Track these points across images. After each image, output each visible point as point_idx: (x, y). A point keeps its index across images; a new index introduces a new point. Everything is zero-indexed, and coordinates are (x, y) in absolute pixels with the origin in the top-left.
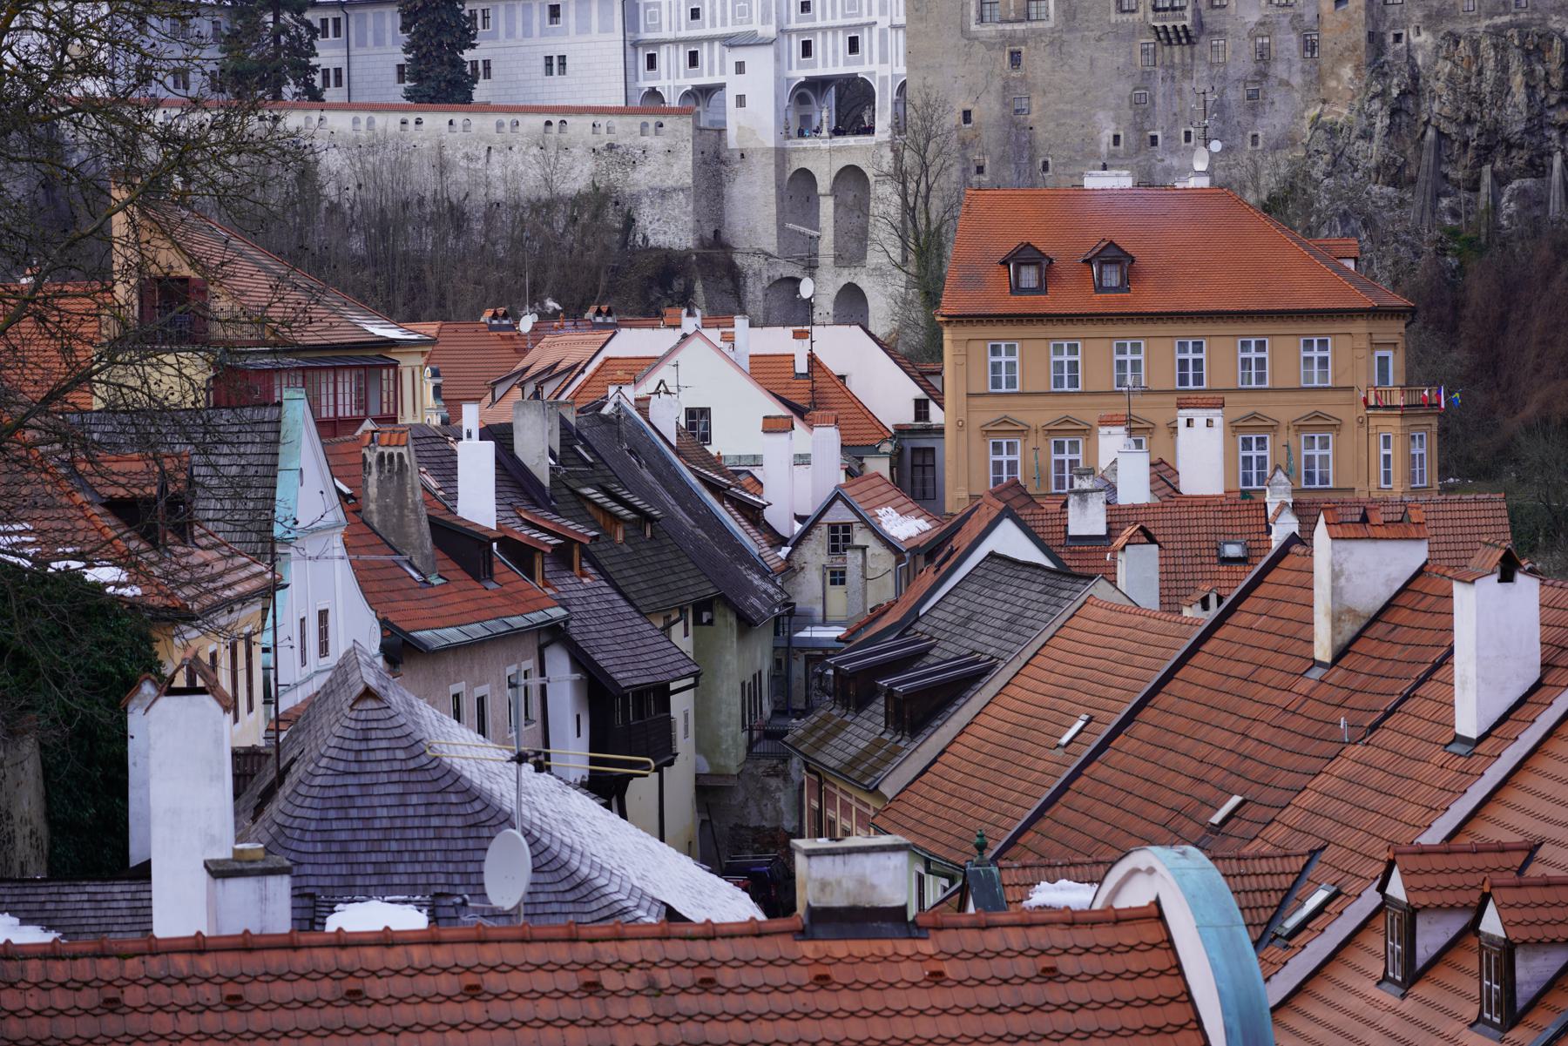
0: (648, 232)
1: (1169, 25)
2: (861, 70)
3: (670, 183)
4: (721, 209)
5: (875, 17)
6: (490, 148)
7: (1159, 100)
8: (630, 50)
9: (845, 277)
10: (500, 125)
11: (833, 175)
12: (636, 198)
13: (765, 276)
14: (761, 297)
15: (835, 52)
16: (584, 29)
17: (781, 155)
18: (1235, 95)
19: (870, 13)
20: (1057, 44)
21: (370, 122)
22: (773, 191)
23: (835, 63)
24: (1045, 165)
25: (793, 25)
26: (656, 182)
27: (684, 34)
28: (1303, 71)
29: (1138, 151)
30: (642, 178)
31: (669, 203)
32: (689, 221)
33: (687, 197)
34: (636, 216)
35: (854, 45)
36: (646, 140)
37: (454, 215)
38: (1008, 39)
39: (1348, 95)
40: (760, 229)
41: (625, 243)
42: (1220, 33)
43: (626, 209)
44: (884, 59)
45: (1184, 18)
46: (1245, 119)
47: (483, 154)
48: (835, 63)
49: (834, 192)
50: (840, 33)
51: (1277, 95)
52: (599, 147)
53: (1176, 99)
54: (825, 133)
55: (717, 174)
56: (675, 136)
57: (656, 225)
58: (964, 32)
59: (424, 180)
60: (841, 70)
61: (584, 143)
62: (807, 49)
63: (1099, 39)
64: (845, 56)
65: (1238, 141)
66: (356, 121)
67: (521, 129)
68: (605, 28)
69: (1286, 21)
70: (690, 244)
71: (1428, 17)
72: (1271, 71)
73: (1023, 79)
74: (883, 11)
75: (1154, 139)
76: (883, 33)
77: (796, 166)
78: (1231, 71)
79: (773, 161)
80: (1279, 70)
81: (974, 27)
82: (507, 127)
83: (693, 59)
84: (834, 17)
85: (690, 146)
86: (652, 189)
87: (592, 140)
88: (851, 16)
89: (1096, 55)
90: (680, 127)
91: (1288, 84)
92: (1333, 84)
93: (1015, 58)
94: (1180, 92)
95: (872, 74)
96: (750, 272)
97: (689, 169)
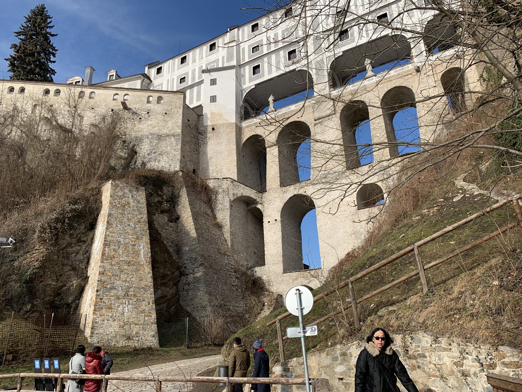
3: (165, 131)
4: (198, 158)
9: (292, 191)
10: (47, 92)
12: (140, 140)
13: (231, 192)
17: (239, 131)
22: (234, 147)
26: (156, 130)
33: (177, 140)
34: (138, 149)
43: (131, 145)
49: (279, 142)
56: (171, 105)
70: (178, 168)
79: (234, 130)
82: (52, 93)
86: (151, 134)
90: (174, 100)
96: (220, 190)
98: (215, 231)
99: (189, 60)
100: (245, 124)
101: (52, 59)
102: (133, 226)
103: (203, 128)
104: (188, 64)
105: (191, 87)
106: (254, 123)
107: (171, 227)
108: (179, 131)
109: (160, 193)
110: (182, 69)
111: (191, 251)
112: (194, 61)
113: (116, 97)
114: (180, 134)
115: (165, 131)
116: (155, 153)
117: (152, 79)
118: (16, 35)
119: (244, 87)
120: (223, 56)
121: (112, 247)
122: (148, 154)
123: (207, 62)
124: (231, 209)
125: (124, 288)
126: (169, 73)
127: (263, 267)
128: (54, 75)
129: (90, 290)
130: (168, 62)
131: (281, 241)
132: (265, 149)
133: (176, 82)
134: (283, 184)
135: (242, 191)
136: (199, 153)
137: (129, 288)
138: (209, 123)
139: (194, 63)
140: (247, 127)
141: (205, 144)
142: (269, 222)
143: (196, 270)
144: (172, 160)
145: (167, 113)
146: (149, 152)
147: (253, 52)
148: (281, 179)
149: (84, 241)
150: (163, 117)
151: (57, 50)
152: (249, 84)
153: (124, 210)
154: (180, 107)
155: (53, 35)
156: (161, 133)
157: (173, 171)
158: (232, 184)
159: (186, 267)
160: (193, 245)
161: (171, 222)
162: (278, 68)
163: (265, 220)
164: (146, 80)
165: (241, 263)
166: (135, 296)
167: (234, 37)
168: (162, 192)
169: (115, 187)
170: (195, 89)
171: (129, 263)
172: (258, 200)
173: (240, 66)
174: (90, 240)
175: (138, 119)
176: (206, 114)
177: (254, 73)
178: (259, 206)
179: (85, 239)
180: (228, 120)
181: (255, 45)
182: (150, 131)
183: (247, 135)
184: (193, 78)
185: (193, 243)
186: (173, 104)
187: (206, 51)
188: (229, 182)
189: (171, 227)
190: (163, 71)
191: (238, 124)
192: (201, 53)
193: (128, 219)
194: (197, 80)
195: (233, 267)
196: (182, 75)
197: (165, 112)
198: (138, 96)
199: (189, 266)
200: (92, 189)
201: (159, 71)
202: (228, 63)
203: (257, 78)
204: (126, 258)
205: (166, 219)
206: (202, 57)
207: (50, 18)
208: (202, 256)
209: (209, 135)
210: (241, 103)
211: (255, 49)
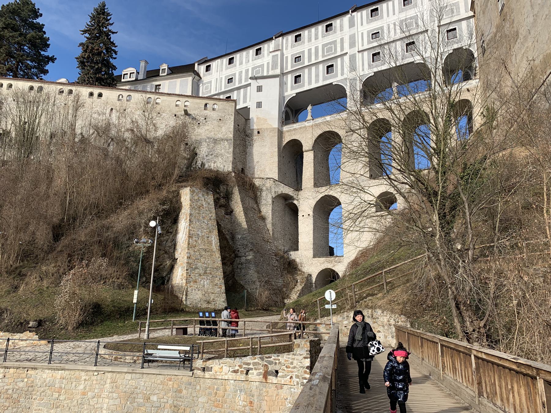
3: (220, 136)
4: (245, 158)
5: (347, 49)
6: (112, 109)
9: (324, 191)
11: (314, 139)
12: (199, 142)
13: (273, 190)
14: (270, 202)
17: (281, 134)
19: (342, 49)
22: (277, 149)
26: (212, 135)
27: (223, 90)
33: (230, 144)
40: (267, 170)
43: (192, 148)
44: (353, 68)
47: (108, 111)
48: (317, 81)
49: (314, 147)
61: (170, 111)
64: (323, 76)
74: (352, 44)
76: (353, 58)
79: (276, 134)
85: (233, 118)
87: (175, 110)
88: (329, 55)
96: (264, 188)
98: (260, 223)
99: (236, 61)
100: (285, 128)
101: (114, 56)
102: (206, 222)
103: (250, 131)
104: (235, 66)
105: (239, 88)
106: (294, 129)
107: (227, 219)
108: (231, 136)
109: (218, 191)
110: (230, 70)
111: (243, 238)
112: (241, 63)
113: (178, 103)
114: (232, 138)
115: (219, 135)
116: (212, 155)
117: (201, 75)
118: (82, 33)
119: (286, 94)
120: (268, 62)
121: (194, 239)
122: (207, 156)
123: (253, 66)
124: (272, 205)
125: (203, 268)
126: (217, 72)
127: (296, 252)
128: (115, 70)
129: (180, 268)
130: (217, 61)
131: (312, 232)
132: (303, 152)
133: (224, 81)
134: (316, 185)
135: (282, 189)
136: (246, 154)
137: (206, 268)
138: (255, 126)
139: (241, 66)
140: (288, 131)
141: (251, 145)
142: (303, 216)
143: (247, 253)
144: (226, 161)
145: (221, 119)
146: (207, 154)
147: (295, 62)
148: (314, 180)
149: (171, 232)
150: (217, 123)
151: (117, 46)
152: (291, 92)
153: (199, 211)
154: (232, 115)
155: (113, 33)
156: (216, 137)
157: (226, 171)
158: (274, 183)
159: (239, 251)
160: (244, 234)
161: (227, 215)
162: (317, 81)
163: (300, 214)
164: (197, 77)
165: (280, 248)
166: (210, 273)
167: (279, 45)
168: (219, 190)
169: (192, 192)
170: (242, 90)
171: (205, 250)
172: (295, 197)
173: (283, 74)
174: (175, 231)
175: (197, 124)
176: (252, 118)
177: (296, 82)
178: (295, 202)
179: (171, 231)
180: (271, 125)
181: (298, 56)
182: (207, 135)
183: (287, 139)
184: (240, 81)
185: (245, 233)
186: (226, 111)
187: (253, 55)
188: (272, 182)
189: (227, 219)
190: (212, 69)
191: (280, 129)
192: (247, 57)
193: (203, 218)
194: (244, 83)
195: (274, 251)
196: (230, 75)
197: (220, 118)
198: (197, 103)
199: (242, 250)
200: (173, 192)
201: (208, 68)
202: (273, 71)
203: (298, 87)
204: (203, 247)
205: (223, 212)
206: (249, 61)
207: (110, 15)
208: (252, 243)
209: (255, 138)
210: (283, 109)
211: (298, 59)
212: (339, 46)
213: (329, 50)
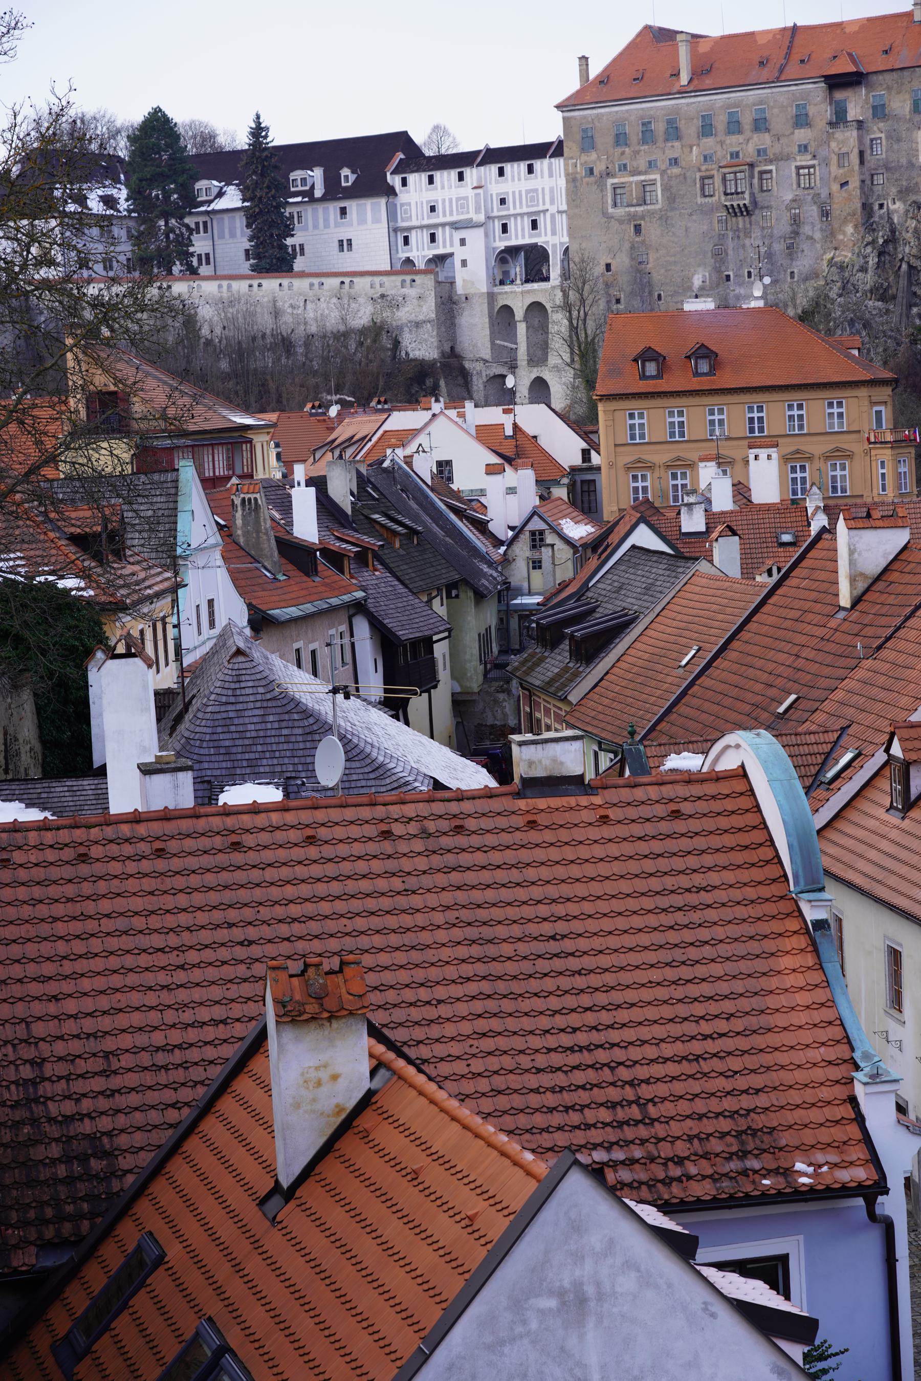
0: (409, 350)
1: (735, 204)
2: (539, 241)
3: (421, 317)
4: (454, 333)
5: (547, 206)
7: (730, 252)
8: (392, 234)
10: (312, 285)
12: (400, 328)
15: (523, 229)
16: (362, 221)
17: (491, 297)
18: (778, 247)
20: (664, 219)
21: (229, 287)
23: (523, 237)
24: (659, 296)
25: (496, 213)
26: (412, 317)
27: (426, 222)
28: (822, 230)
29: (718, 285)
30: (404, 315)
31: (421, 330)
32: (434, 341)
35: (534, 225)
36: (405, 291)
37: (285, 344)
38: (632, 217)
39: (851, 244)
41: (394, 357)
42: (767, 207)
44: (554, 233)
45: (744, 199)
46: (786, 262)
47: (302, 304)
48: (523, 237)
49: (526, 319)
50: (526, 218)
51: (805, 246)
52: (375, 296)
53: (741, 251)
54: (518, 282)
55: (451, 311)
57: (413, 345)
58: (605, 214)
59: (265, 322)
60: (527, 241)
62: (505, 228)
63: (691, 215)
65: (782, 276)
66: (220, 286)
67: (325, 287)
68: (376, 221)
69: (810, 198)
70: (436, 356)
71: (900, 192)
72: (801, 231)
73: (643, 242)
74: (552, 202)
75: (728, 278)
76: (553, 216)
77: (501, 303)
78: (775, 232)
80: (806, 229)
81: (610, 210)
82: (316, 286)
83: (433, 238)
84: (521, 207)
85: (433, 293)
87: (371, 292)
89: (689, 225)
91: (812, 238)
92: (841, 237)
93: (638, 229)
94: (744, 246)
95: (547, 242)
97: (433, 308)
112: (443, 188)
212: (540, 196)
213: (532, 199)
